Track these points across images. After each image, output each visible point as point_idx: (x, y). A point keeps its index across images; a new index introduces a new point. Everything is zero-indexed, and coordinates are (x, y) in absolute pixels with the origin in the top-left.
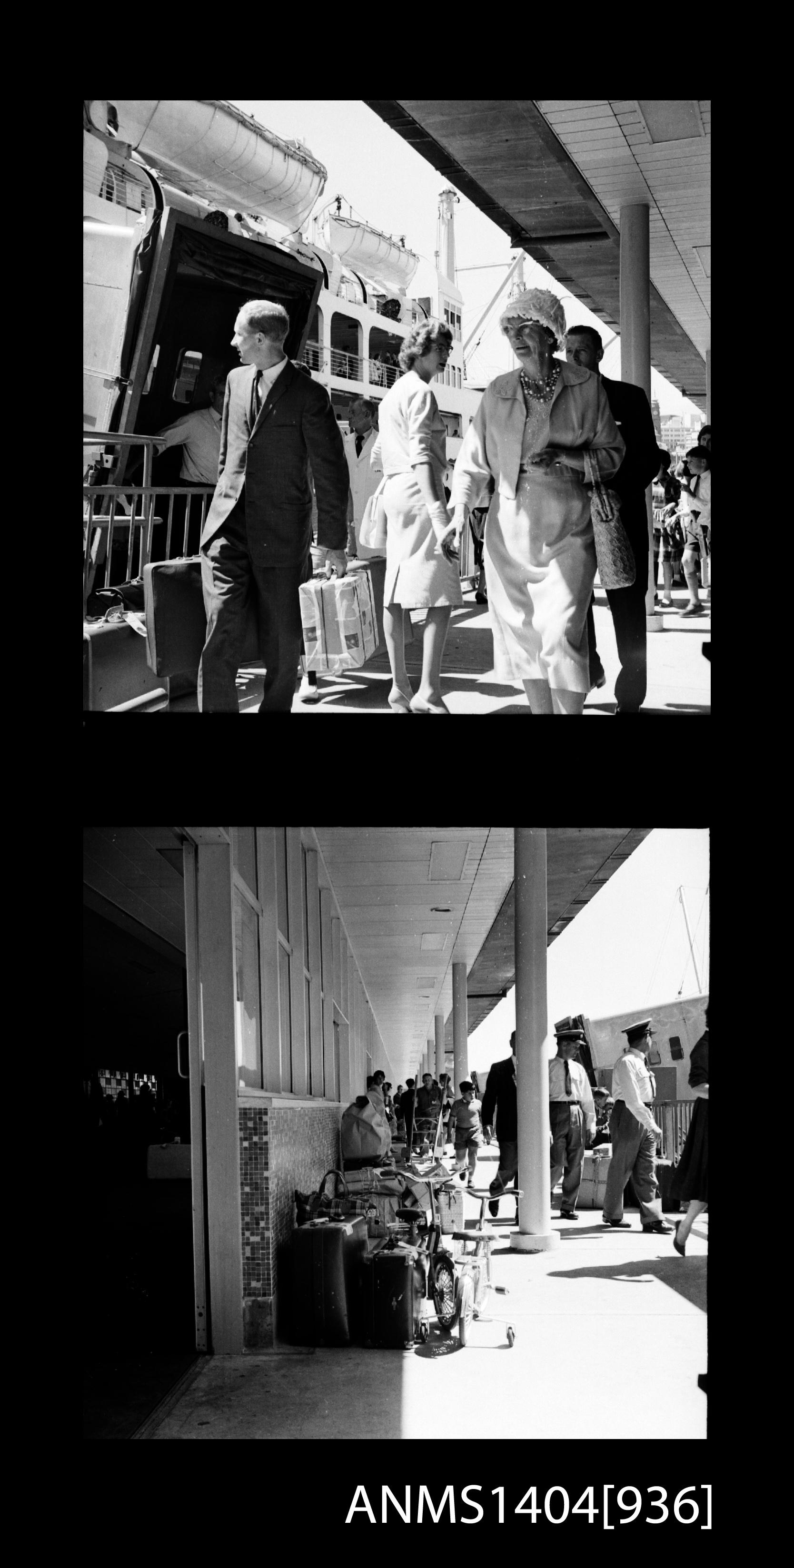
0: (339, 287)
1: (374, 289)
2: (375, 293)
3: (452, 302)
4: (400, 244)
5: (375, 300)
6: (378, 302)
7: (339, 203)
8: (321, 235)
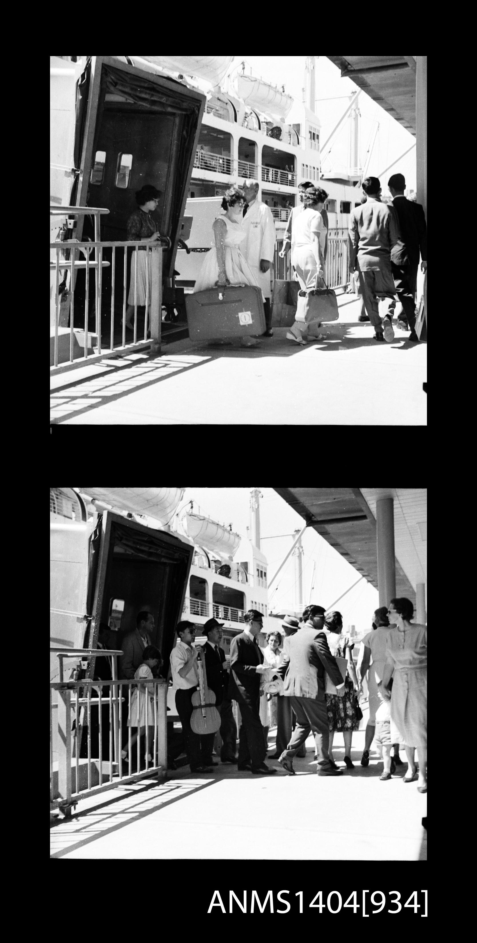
1: (265, 118)
7: (244, 65)
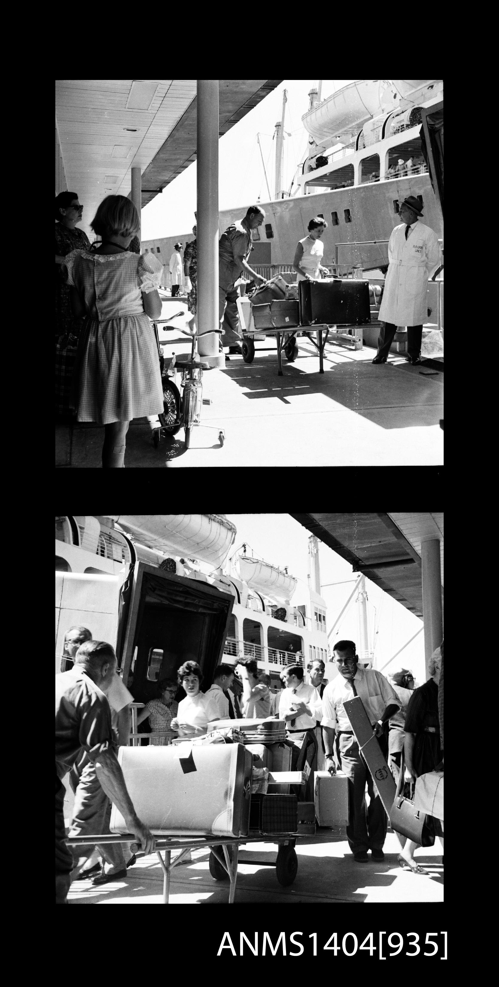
0: (247, 601)
1: (269, 602)
2: (270, 604)
3: (319, 607)
4: (285, 572)
5: (270, 609)
6: (272, 610)
7: (245, 548)
8: (234, 569)
